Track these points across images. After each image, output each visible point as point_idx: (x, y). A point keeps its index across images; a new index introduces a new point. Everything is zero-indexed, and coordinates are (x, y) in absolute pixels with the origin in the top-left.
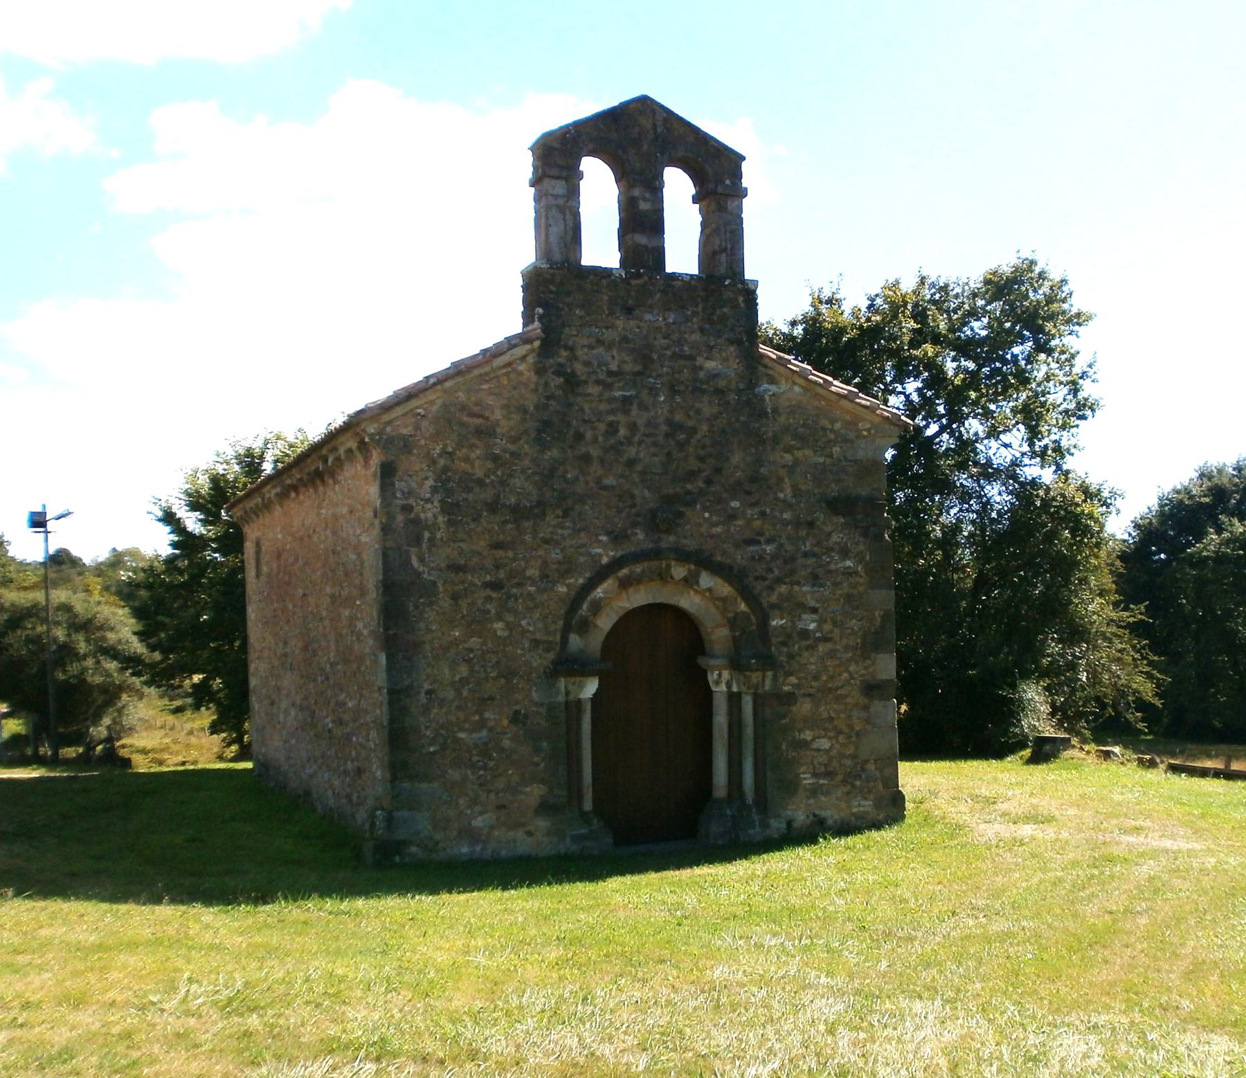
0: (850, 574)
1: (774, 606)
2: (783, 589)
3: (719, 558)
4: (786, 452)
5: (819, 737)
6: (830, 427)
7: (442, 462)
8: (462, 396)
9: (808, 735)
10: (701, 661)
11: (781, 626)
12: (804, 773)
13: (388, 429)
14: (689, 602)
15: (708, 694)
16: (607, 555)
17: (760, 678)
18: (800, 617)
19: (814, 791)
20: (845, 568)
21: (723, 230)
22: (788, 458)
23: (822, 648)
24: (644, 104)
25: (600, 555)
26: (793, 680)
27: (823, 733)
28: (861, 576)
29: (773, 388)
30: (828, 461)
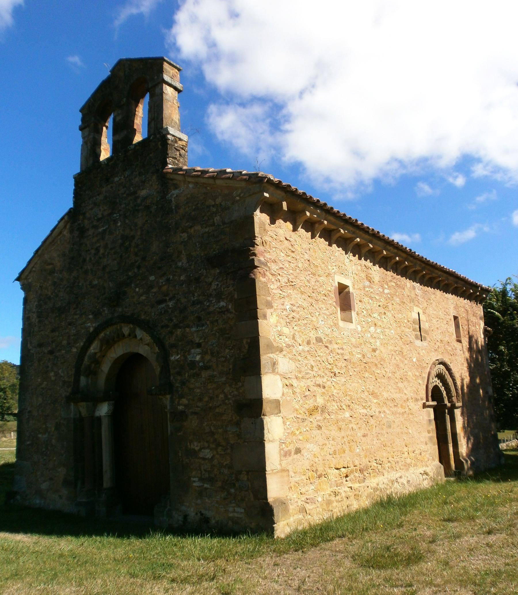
0: (223, 312)
1: (173, 346)
2: (179, 332)
3: (143, 317)
4: (182, 233)
5: (204, 448)
6: (213, 203)
9: (195, 446)
11: (177, 360)
12: (195, 477)
16: (92, 326)
18: (189, 351)
19: (201, 493)
20: (220, 308)
22: (185, 235)
23: (205, 374)
26: (184, 401)
27: (206, 445)
28: (231, 313)
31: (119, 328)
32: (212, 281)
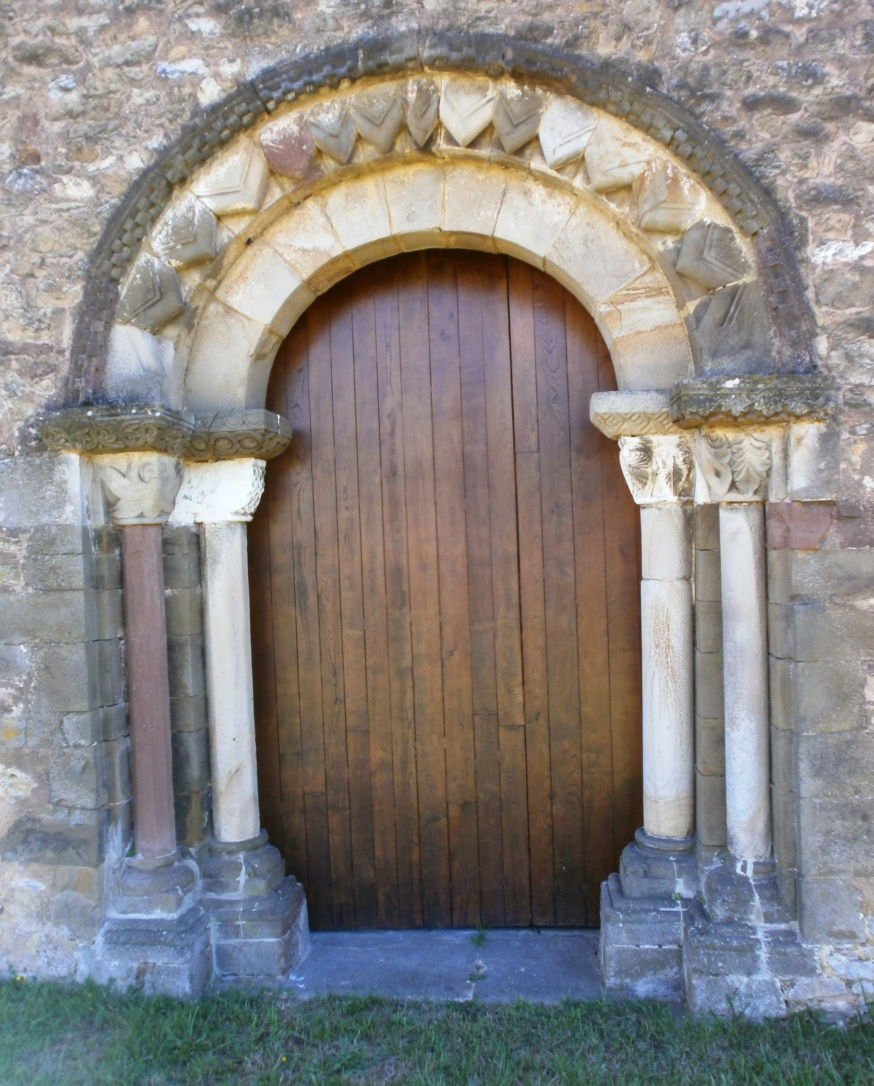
16: (217, 76)
17: (776, 446)
25: (195, 79)
31: (412, 96)
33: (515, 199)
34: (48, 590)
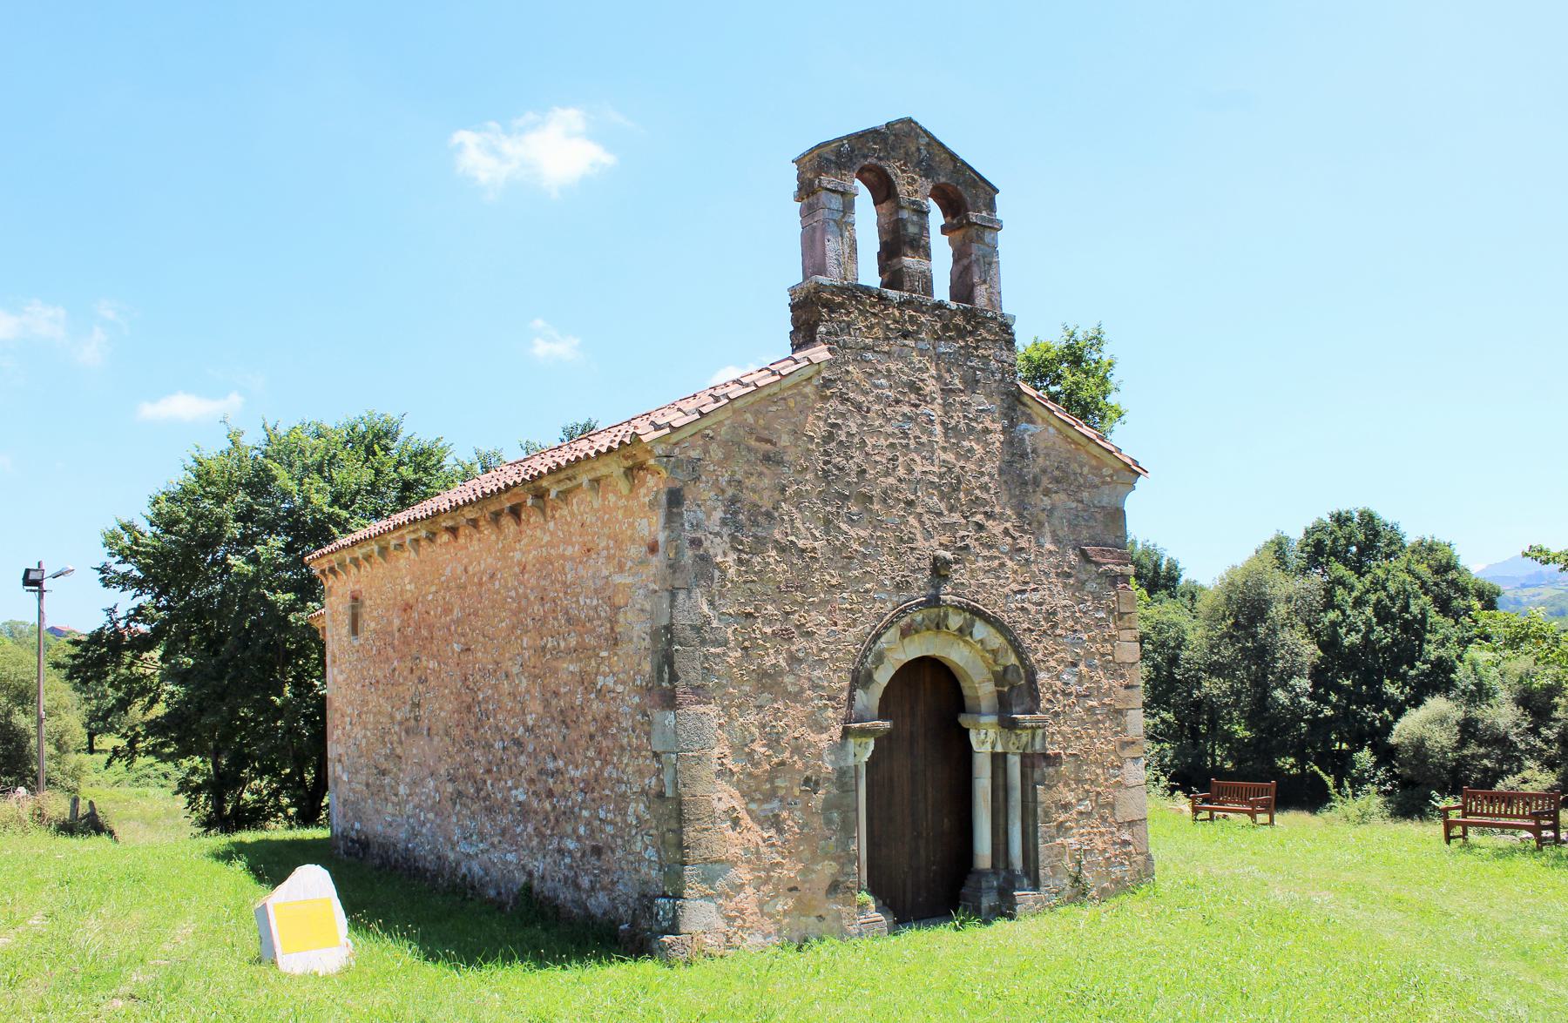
7: (730, 492)
8: (749, 418)
10: (965, 720)
13: (677, 451)
14: (957, 655)
15: (967, 753)
21: (982, 260)
24: (910, 120)
29: (1031, 426)
30: (1080, 505)
32: (1087, 581)
33: (956, 646)
34: (843, 792)
